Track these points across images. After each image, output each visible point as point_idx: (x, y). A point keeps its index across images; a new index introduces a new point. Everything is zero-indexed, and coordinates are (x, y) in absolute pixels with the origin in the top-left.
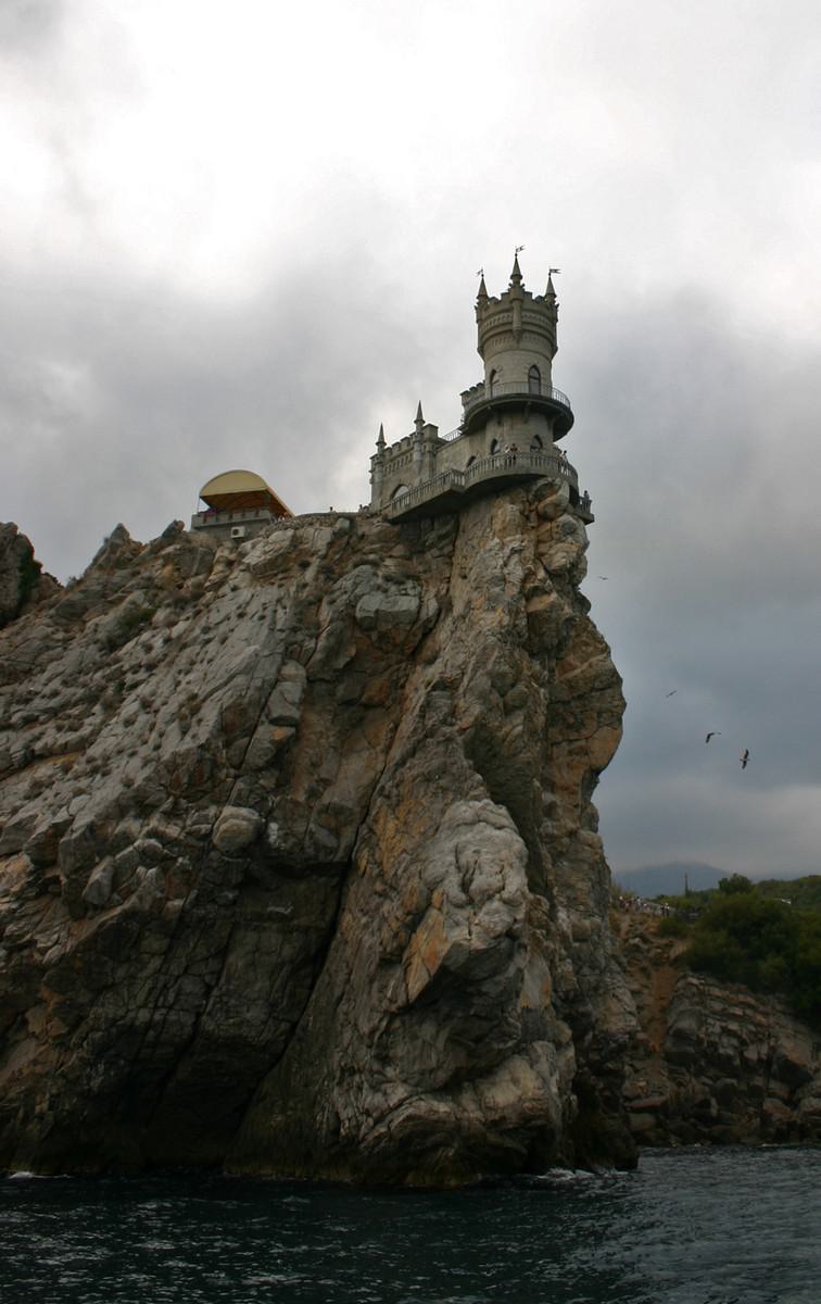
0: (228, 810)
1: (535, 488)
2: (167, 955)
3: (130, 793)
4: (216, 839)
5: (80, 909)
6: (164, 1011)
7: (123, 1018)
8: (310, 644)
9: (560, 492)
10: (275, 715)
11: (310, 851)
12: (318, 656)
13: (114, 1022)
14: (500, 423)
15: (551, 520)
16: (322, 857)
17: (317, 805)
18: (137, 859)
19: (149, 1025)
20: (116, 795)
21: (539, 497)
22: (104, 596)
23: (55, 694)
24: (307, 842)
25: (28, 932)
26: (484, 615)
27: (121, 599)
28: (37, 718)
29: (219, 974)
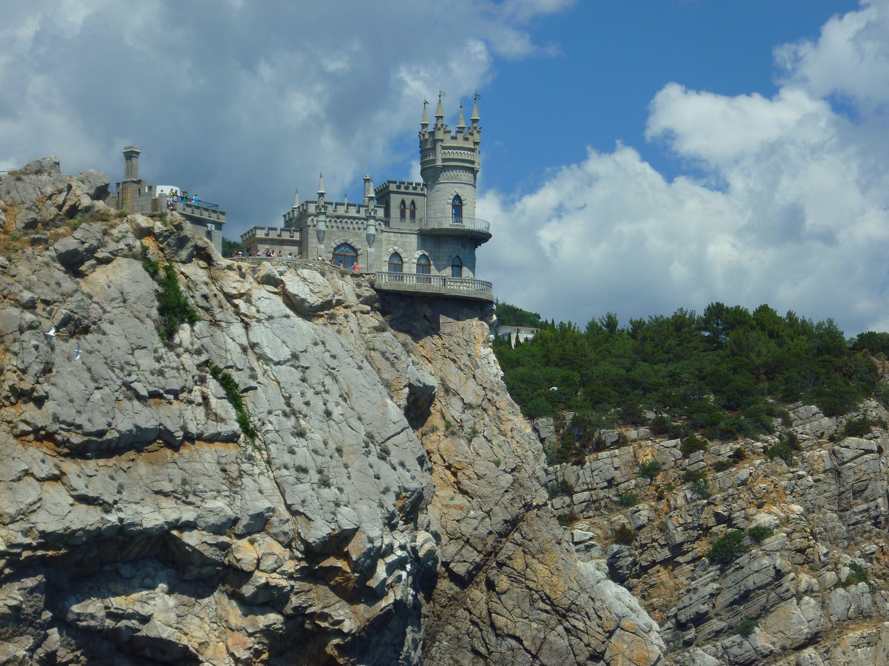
4: (421, 554)
5: (360, 592)
25: (311, 606)
26: (510, 417)
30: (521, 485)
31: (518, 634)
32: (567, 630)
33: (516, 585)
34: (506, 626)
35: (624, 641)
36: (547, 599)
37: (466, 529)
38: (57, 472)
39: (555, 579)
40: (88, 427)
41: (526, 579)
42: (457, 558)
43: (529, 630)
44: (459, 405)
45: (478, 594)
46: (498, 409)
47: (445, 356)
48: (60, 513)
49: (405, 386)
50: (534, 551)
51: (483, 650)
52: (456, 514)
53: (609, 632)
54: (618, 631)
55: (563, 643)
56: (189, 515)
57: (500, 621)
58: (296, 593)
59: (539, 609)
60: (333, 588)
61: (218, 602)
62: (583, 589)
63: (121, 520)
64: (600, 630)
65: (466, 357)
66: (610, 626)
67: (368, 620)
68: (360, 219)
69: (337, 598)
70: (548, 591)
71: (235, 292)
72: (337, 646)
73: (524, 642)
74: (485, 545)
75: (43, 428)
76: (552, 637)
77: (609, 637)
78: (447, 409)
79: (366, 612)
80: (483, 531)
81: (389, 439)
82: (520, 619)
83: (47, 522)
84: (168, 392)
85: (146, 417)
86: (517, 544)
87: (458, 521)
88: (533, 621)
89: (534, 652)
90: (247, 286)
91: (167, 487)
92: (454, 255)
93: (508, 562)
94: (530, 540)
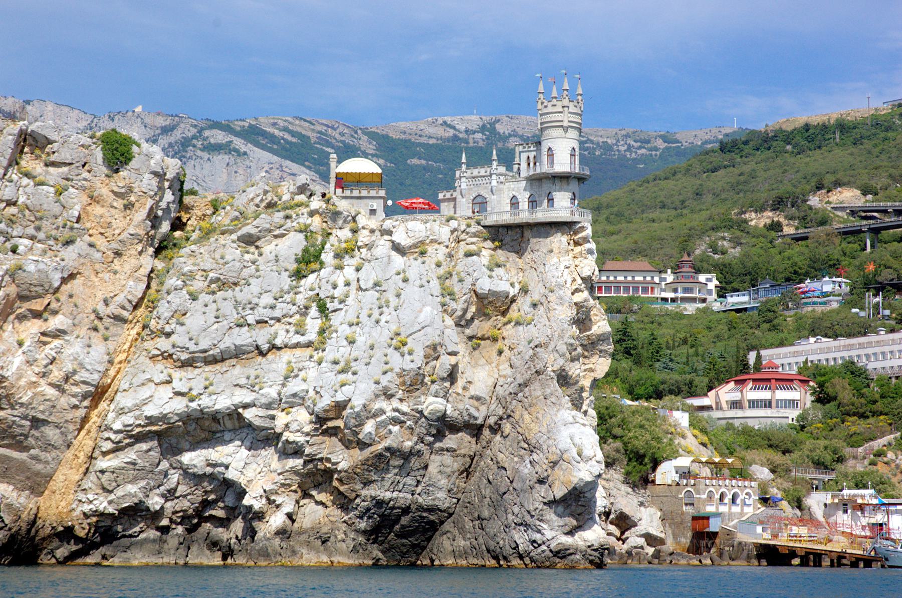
0: (431, 399)
3: (380, 387)
4: (426, 413)
5: (354, 442)
8: (453, 305)
10: (450, 351)
11: (466, 418)
12: (459, 313)
13: (373, 498)
15: (580, 245)
16: (471, 421)
17: (468, 394)
19: (391, 500)
20: (373, 388)
23: (273, 307)
24: (465, 414)
26: (556, 307)
28: (266, 322)
36: (526, 441)
38: (168, 379)
40: (193, 348)
45: (498, 437)
48: (165, 403)
51: (491, 478)
54: (561, 462)
55: (526, 471)
56: (248, 397)
57: (501, 456)
60: (340, 440)
61: (269, 455)
63: (199, 406)
64: (546, 461)
65: (542, 266)
66: (554, 458)
72: (337, 479)
75: (165, 352)
77: (553, 468)
78: (523, 306)
79: (358, 455)
83: (151, 410)
84: (272, 319)
85: (243, 337)
90: (374, 238)
91: (243, 381)
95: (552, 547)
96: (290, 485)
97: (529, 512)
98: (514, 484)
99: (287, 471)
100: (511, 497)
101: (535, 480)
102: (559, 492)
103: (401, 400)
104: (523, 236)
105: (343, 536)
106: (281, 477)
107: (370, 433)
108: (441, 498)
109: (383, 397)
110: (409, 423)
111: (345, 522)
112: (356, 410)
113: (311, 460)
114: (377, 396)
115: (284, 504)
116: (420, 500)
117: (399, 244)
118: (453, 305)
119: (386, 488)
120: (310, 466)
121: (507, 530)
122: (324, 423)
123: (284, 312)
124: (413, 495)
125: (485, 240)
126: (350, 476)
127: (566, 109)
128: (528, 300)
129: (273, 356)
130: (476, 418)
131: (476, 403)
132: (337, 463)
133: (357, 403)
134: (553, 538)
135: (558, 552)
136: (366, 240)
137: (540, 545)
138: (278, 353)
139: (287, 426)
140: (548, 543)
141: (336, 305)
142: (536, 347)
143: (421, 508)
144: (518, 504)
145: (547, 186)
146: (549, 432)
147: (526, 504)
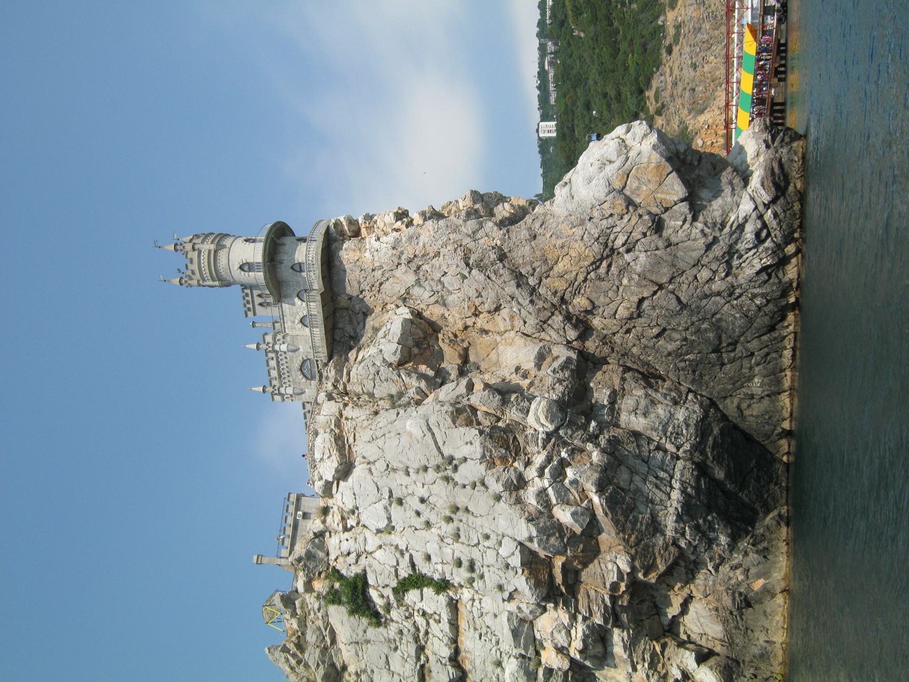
0: (531, 420)
1: (334, 235)
2: (633, 471)
3: (505, 495)
4: (551, 427)
6: (673, 481)
7: (676, 509)
8: (412, 392)
9: (342, 219)
12: (423, 385)
13: (679, 518)
14: (281, 263)
15: (359, 229)
18: (559, 485)
19: (683, 491)
20: (506, 506)
21: (342, 233)
22: (326, 648)
24: (560, 375)
25: (603, 600)
26: (421, 244)
27: (333, 633)
29: (650, 440)
30: (481, 261)
31: (635, 299)
32: (628, 251)
33: (582, 291)
34: (628, 308)
35: (638, 188)
36: (596, 264)
37: (532, 321)
39: (573, 253)
41: (576, 280)
42: (562, 333)
43: (630, 292)
44: (416, 291)
45: (596, 322)
46: (415, 256)
47: (379, 291)
49: (399, 376)
50: (545, 268)
51: (655, 331)
52: (518, 323)
53: (627, 208)
54: (627, 192)
55: (642, 257)
57: (622, 312)
58: (591, 615)
59: (607, 273)
60: (585, 565)
62: (582, 223)
64: (626, 218)
66: (620, 203)
67: (618, 534)
68: (277, 358)
69: (596, 561)
70: (587, 263)
71: (341, 525)
72: (645, 575)
73: (645, 295)
74: (545, 309)
76: (638, 269)
77: (636, 206)
79: (608, 537)
80: (530, 308)
81: (438, 448)
82: (620, 294)
84: (418, 659)
86: (540, 284)
87: (525, 322)
88: (620, 281)
89: (657, 288)
90: (335, 508)
92: (291, 271)
93: (559, 294)
94: (534, 270)
95: (766, 197)
96: (654, 655)
97: (709, 247)
98: (664, 280)
99: (630, 656)
100: (685, 287)
101: (655, 237)
102: (675, 189)
103: (528, 463)
104: (347, 309)
105: (738, 572)
106: (639, 667)
107: (573, 514)
108: (686, 414)
109: (522, 492)
110: (564, 454)
111: (716, 568)
112: (534, 533)
113: (613, 615)
114: (519, 501)
115: (682, 667)
116: (687, 446)
117: (337, 471)
118: (412, 392)
119: (664, 497)
120: (624, 617)
121: (738, 291)
122: (557, 588)
123: (411, 640)
124: (678, 458)
125: (347, 360)
126: (641, 554)
127: (196, 247)
128: (416, 291)
129: (467, 662)
130: (569, 360)
131: (549, 360)
132: (619, 571)
133: (524, 530)
134: (752, 199)
135: (776, 185)
136: (338, 518)
137: (765, 225)
138: (463, 654)
139: (560, 650)
140: (761, 208)
141: (405, 562)
142: (467, 265)
143: (699, 447)
144: (694, 271)
145: (285, 272)
146: (582, 223)
147: (696, 255)
